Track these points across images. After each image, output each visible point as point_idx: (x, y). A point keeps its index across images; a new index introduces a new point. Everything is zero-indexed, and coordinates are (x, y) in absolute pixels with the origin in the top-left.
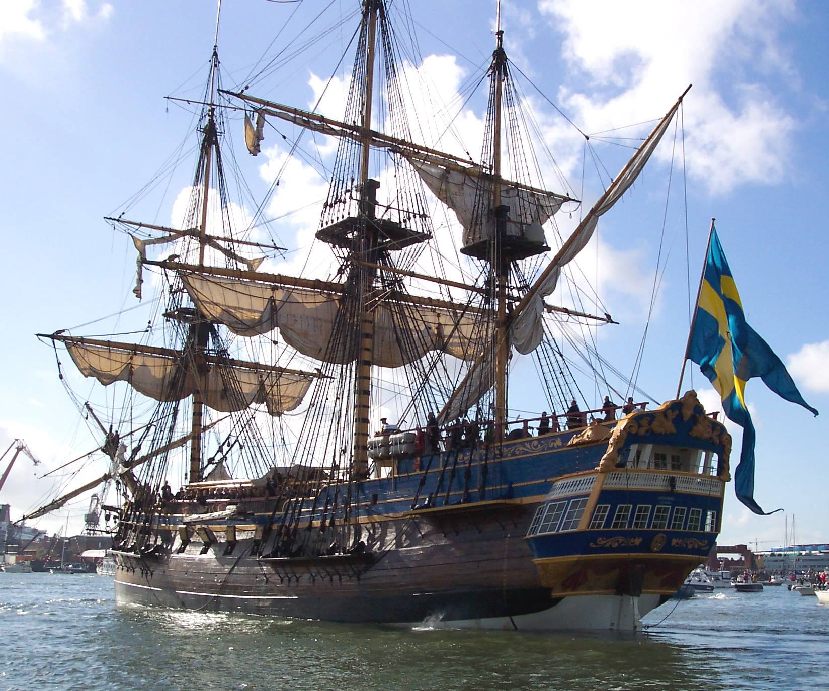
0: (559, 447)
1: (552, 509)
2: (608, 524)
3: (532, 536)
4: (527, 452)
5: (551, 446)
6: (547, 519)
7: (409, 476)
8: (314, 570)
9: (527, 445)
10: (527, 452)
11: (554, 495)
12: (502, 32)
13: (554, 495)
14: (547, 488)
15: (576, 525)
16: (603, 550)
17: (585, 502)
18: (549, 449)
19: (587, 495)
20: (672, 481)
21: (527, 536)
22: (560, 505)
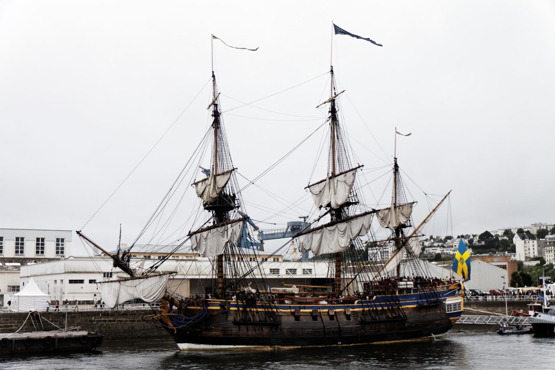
4: (439, 290)
8: (371, 325)
13: (447, 302)
19: (461, 302)
21: (447, 312)
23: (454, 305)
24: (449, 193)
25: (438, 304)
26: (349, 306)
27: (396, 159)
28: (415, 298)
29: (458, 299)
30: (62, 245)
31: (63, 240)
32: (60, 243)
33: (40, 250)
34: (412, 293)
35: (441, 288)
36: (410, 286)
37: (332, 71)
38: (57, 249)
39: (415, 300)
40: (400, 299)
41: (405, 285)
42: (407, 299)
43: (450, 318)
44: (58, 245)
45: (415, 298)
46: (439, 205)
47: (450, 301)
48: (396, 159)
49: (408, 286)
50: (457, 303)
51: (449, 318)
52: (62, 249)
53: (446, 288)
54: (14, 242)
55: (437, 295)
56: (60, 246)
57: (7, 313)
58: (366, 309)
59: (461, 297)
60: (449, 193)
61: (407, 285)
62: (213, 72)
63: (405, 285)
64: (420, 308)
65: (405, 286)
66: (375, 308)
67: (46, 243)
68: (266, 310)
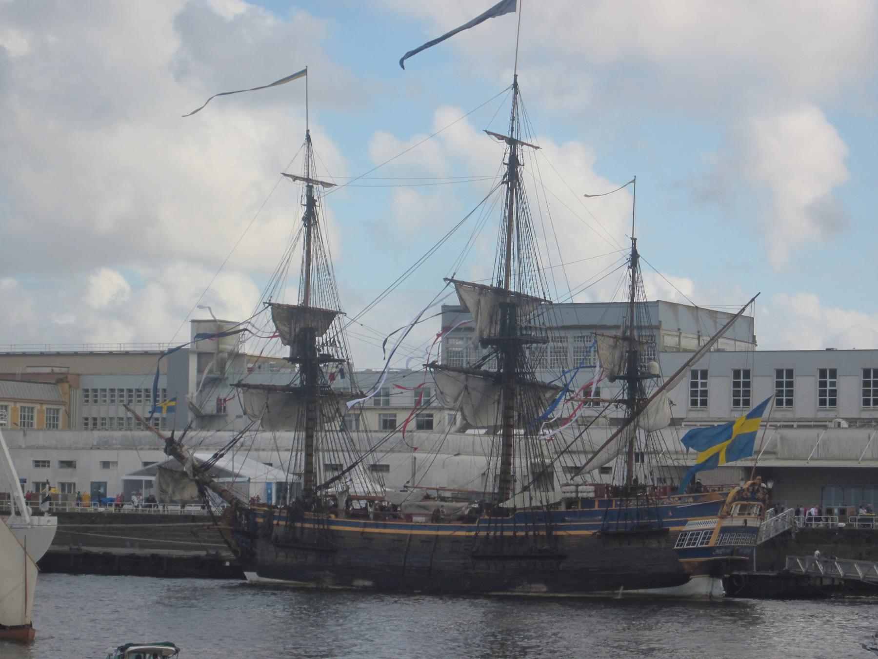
0: (691, 502)
1: (692, 535)
2: (720, 543)
3: (679, 548)
4: (671, 503)
5: (686, 501)
6: (690, 539)
7: (591, 511)
9: (671, 499)
10: (671, 503)
12: (635, 240)
14: (684, 523)
15: (707, 543)
16: (717, 555)
17: (711, 533)
18: (685, 503)
19: (714, 529)
20: (745, 521)
21: (675, 547)
24: (753, 300)
25: (663, 533)
26: (464, 527)
27: (635, 240)
28: (600, 517)
29: (708, 523)
30: (833, 384)
31: (833, 373)
32: (828, 380)
34: (596, 508)
35: (677, 499)
36: (585, 494)
37: (515, 85)
38: (822, 393)
39: (600, 521)
40: (567, 518)
41: (571, 492)
42: (582, 519)
43: (682, 560)
44: (823, 384)
45: (600, 517)
46: (725, 327)
47: (696, 524)
48: (634, 240)
49: (580, 495)
50: (703, 530)
51: (679, 560)
52: (834, 393)
53: (691, 500)
54: (731, 379)
55: (659, 513)
57: (158, 513)
58: (483, 533)
59: (717, 520)
60: (753, 300)
61: (577, 492)
62: (308, 131)
63: (571, 492)
64: (606, 535)
65: (574, 495)
66: (498, 533)
68: (316, 526)
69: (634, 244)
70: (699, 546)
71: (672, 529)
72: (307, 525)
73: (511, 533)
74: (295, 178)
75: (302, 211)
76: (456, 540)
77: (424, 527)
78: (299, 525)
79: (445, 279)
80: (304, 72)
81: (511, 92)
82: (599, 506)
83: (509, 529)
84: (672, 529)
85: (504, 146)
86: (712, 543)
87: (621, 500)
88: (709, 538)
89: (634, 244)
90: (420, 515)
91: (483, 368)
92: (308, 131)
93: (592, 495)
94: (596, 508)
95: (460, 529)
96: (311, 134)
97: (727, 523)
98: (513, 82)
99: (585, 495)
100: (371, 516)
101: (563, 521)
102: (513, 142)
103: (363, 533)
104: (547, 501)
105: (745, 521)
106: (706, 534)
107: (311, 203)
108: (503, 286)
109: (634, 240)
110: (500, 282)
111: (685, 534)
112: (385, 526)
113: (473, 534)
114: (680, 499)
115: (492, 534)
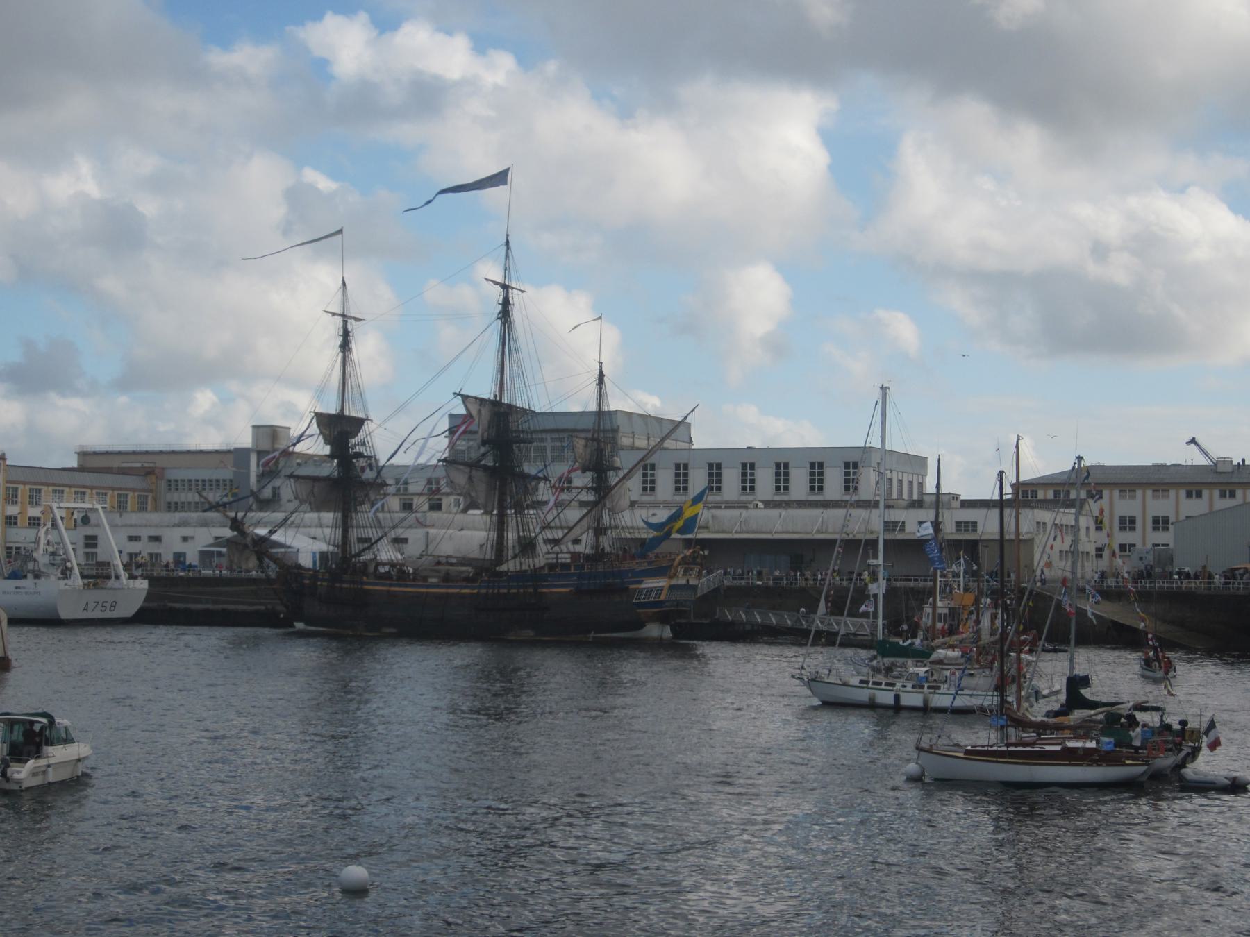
6: (646, 595)
11: (643, 586)
13: (643, 586)
14: (640, 582)
15: (659, 597)
16: (667, 607)
17: (662, 590)
20: (688, 581)
22: (651, 590)
23: (647, 591)
30: (752, 474)
31: (752, 466)
32: (749, 471)
33: (782, 485)
34: (572, 571)
37: (507, 243)
38: (744, 481)
43: (639, 611)
44: (744, 474)
47: (651, 583)
49: (559, 561)
52: (753, 481)
53: (646, 564)
54: (673, 471)
56: (749, 477)
58: (484, 591)
61: (557, 558)
65: (555, 561)
66: (496, 591)
67: (691, 472)
68: (352, 586)
69: (601, 367)
70: (653, 600)
71: (632, 586)
72: (345, 586)
73: (505, 591)
74: (334, 314)
75: (339, 340)
76: (463, 596)
77: (437, 586)
78: (338, 585)
79: (455, 393)
80: (340, 231)
81: (505, 248)
82: (575, 569)
83: (504, 587)
84: (632, 586)
85: (499, 290)
86: (662, 598)
87: (592, 565)
88: (660, 594)
89: (601, 367)
90: (435, 577)
91: (483, 462)
92: (343, 278)
93: (569, 561)
94: (572, 571)
95: (466, 587)
96: (345, 280)
97: (674, 582)
98: (505, 240)
99: (563, 561)
100: (395, 578)
101: (547, 581)
102: (505, 287)
103: (388, 591)
104: (534, 566)
105: (688, 581)
106: (658, 590)
107: (346, 334)
108: (498, 399)
109: (601, 363)
110: (496, 396)
111: (641, 590)
112: (406, 586)
113: (476, 591)
114: (637, 563)
115: (491, 591)
